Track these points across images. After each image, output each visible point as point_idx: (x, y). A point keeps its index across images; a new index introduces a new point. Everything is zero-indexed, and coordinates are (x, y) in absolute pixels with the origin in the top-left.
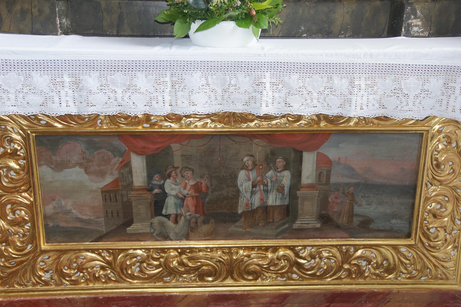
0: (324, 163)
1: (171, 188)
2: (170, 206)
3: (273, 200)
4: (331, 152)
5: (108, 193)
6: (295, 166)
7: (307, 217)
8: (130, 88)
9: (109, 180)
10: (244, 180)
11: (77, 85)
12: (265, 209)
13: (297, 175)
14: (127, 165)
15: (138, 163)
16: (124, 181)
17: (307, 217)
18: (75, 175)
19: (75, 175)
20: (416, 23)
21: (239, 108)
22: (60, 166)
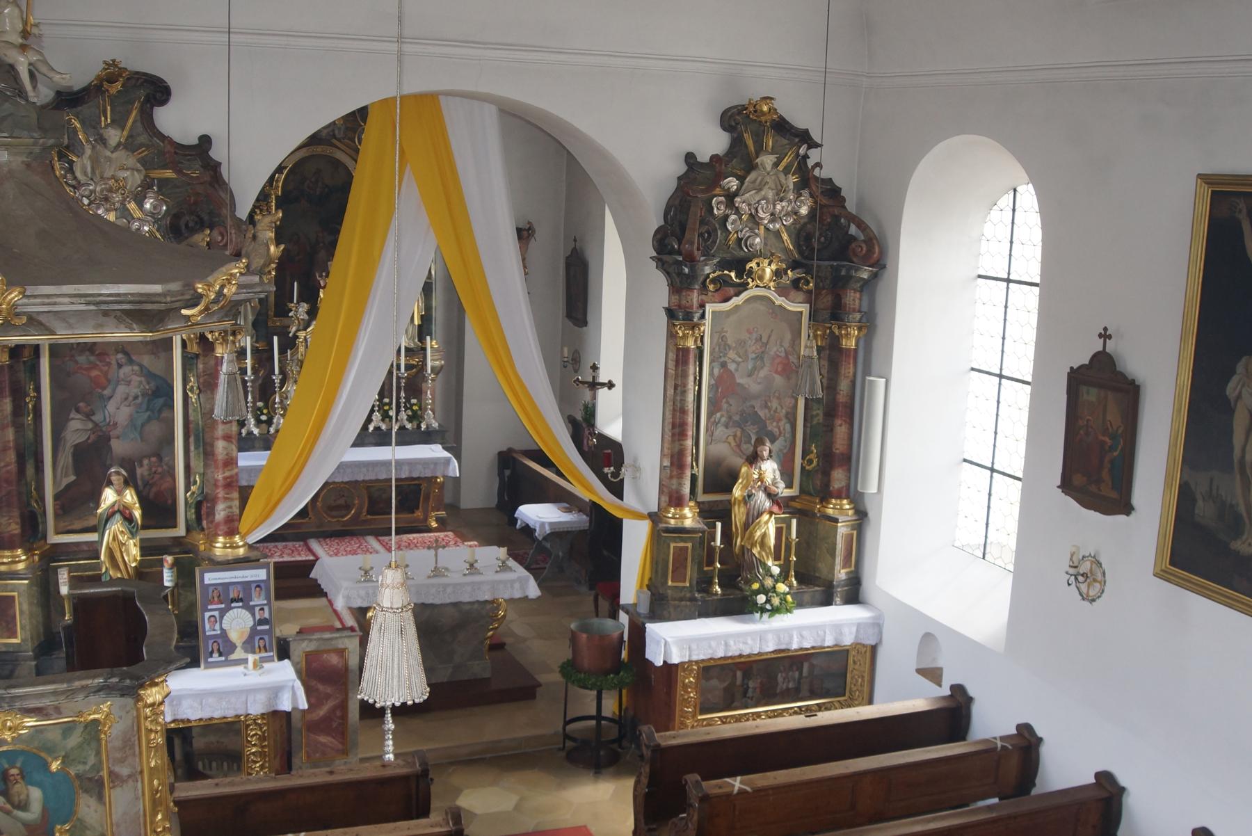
0: (812, 666)
1: (751, 684)
2: (750, 694)
3: (791, 685)
4: (815, 662)
5: (725, 689)
6: (800, 669)
7: (805, 692)
8: (745, 643)
9: (726, 684)
10: (780, 678)
11: (726, 645)
12: (788, 689)
13: (801, 673)
14: (735, 676)
15: (739, 674)
16: (733, 684)
17: (805, 692)
18: (714, 682)
19: (714, 682)
20: (838, 600)
21: (783, 647)
22: (708, 679)
